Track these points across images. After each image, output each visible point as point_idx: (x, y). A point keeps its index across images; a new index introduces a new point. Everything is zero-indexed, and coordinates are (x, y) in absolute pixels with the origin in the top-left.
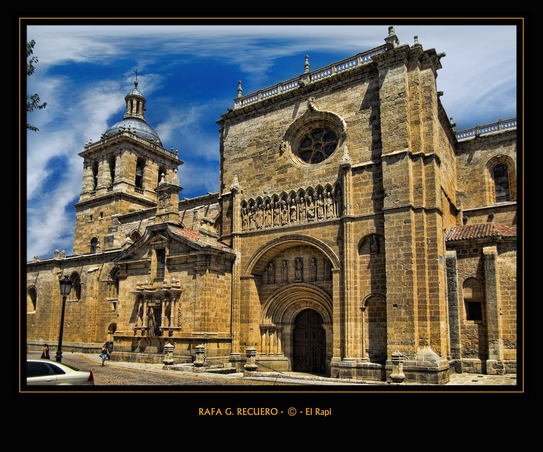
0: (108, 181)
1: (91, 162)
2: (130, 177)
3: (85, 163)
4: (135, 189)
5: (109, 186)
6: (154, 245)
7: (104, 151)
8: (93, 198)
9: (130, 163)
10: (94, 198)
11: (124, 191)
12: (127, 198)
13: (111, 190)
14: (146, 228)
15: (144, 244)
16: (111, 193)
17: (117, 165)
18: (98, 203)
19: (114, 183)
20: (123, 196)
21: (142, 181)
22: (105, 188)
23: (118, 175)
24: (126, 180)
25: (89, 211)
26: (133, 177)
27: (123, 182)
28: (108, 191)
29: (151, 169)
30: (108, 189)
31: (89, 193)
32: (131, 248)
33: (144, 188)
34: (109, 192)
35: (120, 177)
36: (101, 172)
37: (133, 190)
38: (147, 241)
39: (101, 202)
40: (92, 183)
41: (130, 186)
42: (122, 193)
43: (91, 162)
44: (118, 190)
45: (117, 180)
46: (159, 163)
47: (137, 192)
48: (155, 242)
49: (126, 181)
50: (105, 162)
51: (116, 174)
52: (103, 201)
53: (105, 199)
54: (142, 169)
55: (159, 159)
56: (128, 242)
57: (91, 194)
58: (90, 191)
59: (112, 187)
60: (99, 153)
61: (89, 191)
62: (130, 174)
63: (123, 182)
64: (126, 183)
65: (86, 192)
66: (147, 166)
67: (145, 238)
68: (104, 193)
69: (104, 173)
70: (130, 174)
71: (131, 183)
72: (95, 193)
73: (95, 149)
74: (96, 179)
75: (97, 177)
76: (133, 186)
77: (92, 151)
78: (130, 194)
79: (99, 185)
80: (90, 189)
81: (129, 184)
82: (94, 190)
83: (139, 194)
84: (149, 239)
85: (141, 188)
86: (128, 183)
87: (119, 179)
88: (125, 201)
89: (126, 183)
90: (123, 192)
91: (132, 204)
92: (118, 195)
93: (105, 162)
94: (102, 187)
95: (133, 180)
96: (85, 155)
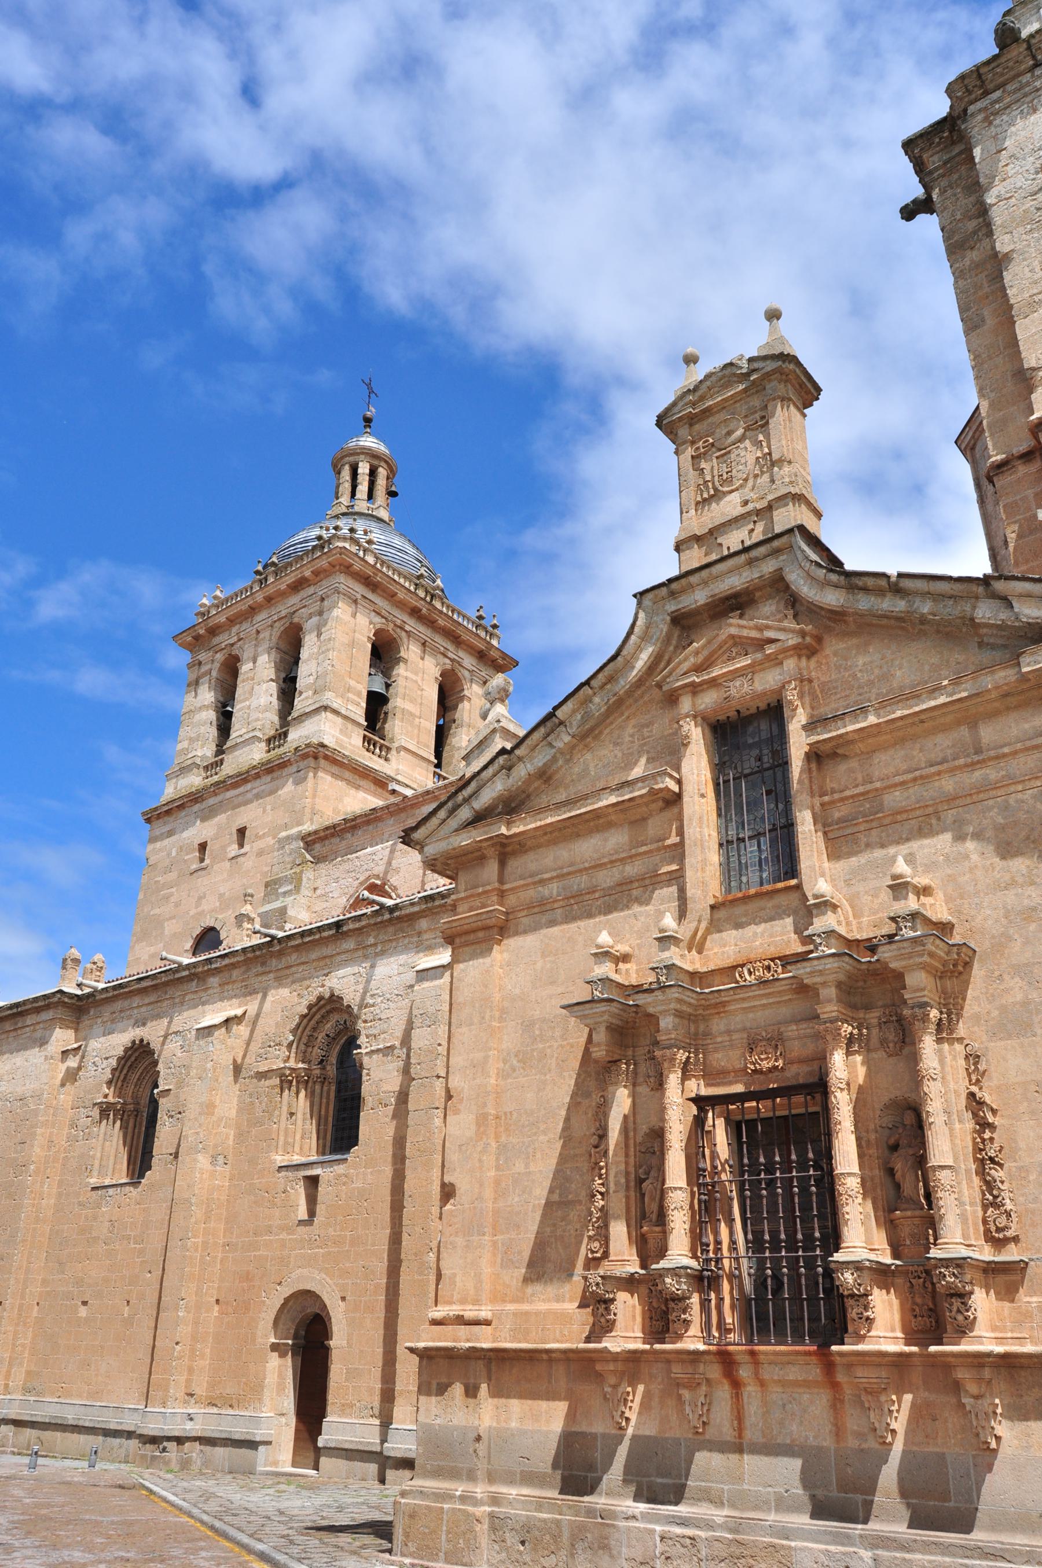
0: (268, 715)
2: (350, 695)
4: (365, 737)
5: (272, 733)
6: (695, 689)
9: (352, 644)
11: (328, 741)
12: (335, 769)
14: (639, 604)
17: (304, 654)
20: (326, 757)
22: (259, 740)
23: (308, 687)
25: (197, 831)
26: (359, 694)
27: (326, 708)
28: (269, 751)
29: (416, 674)
30: (269, 741)
31: (198, 766)
32: (537, 736)
33: (392, 740)
34: (272, 752)
35: (315, 692)
36: (247, 688)
38: (640, 682)
39: (241, 789)
40: (213, 732)
41: (350, 726)
42: (323, 745)
45: (302, 703)
46: (440, 656)
47: (368, 750)
48: (698, 669)
49: (335, 706)
52: (249, 786)
53: (257, 776)
54: (387, 673)
55: (441, 642)
57: (206, 768)
58: (203, 757)
59: (285, 734)
61: (198, 761)
62: (353, 683)
63: (326, 708)
64: (336, 712)
65: (189, 762)
66: (406, 661)
67: (629, 665)
68: (257, 754)
69: (256, 687)
70: (353, 683)
71: (352, 716)
76: (359, 724)
79: (238, 730)
80: (206, 751)
81: (346, 718)
83: (375, 758)
86: (343, 712)
87: (310, 701)
88: (329, 778)
89: (336, 712)
90: (326, 742)
94: (247, 737)
95: (358, 704)
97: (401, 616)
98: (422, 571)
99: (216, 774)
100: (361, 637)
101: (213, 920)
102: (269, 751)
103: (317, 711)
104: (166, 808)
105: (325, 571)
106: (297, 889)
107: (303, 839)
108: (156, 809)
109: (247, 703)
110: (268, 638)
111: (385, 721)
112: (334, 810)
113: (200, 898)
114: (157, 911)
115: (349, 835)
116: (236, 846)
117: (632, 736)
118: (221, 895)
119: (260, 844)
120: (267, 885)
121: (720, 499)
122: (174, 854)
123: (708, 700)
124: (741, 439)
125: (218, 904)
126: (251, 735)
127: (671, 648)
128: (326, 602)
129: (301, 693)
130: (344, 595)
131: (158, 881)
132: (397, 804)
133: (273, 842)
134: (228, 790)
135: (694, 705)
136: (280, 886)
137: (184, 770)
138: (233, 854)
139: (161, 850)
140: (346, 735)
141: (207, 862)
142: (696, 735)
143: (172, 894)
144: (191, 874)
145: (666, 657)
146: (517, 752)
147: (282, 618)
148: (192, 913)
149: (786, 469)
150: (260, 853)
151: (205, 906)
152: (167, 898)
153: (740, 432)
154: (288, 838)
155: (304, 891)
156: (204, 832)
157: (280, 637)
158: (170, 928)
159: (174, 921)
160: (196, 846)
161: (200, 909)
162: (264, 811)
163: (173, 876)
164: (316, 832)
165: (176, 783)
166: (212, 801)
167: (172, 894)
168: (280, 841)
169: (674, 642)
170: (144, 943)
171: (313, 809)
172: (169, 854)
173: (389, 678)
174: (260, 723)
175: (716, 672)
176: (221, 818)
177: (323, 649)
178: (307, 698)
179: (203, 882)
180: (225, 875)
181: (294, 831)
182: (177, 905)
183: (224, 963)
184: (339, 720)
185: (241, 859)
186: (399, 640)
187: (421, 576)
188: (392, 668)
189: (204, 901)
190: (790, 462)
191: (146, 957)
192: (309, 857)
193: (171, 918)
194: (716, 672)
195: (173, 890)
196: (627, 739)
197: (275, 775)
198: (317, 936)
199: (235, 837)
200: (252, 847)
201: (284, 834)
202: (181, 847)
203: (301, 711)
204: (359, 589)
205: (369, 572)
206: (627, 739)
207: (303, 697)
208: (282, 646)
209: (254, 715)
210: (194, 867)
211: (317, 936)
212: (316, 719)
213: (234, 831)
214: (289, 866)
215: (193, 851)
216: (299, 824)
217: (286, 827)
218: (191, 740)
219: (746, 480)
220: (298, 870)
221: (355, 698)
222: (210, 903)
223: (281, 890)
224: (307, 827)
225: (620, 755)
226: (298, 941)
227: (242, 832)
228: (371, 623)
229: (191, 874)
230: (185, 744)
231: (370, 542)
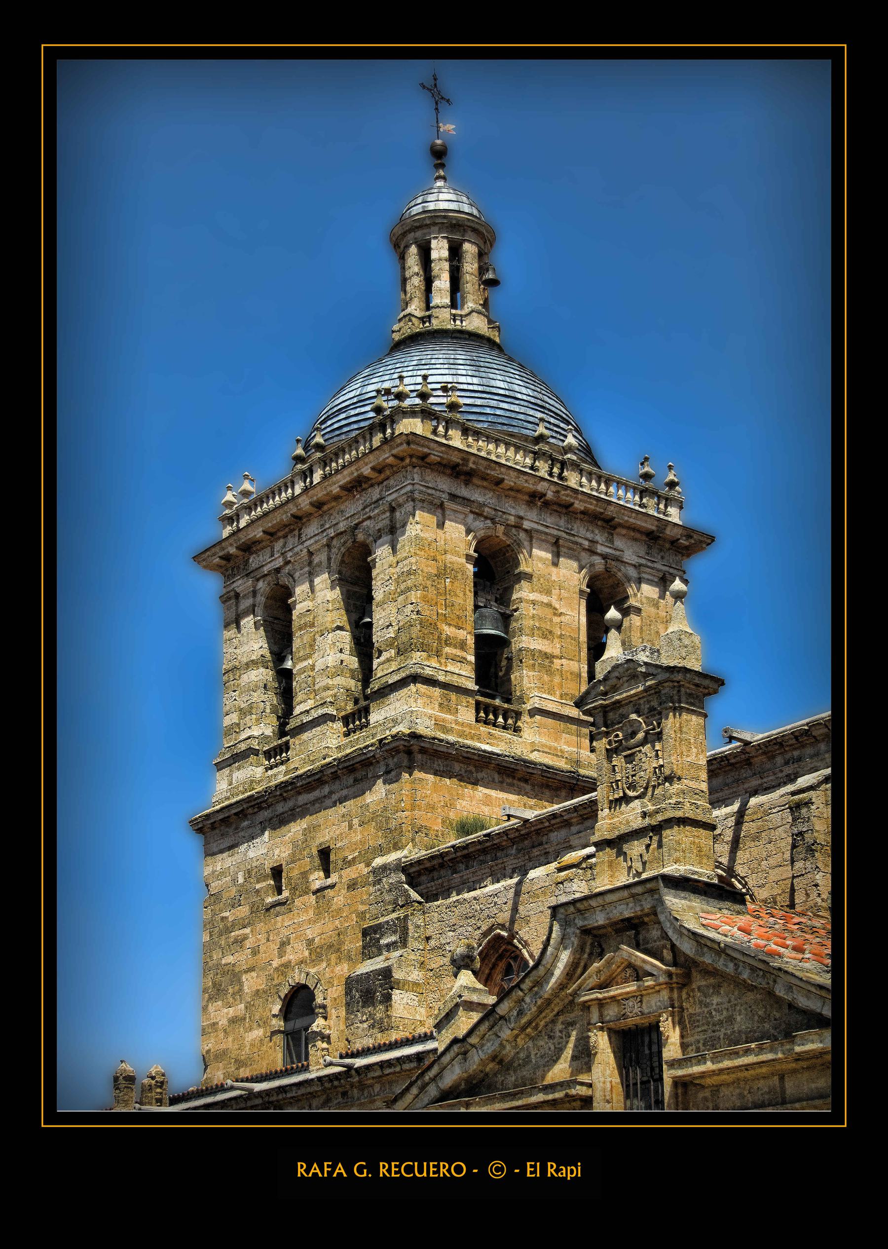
0: (339, 680)
1: (254, 593)
2: (447, 650)
3: (230, 598)
5: (350, 707)
7: (312, 529)
8: (280, 775)
10: (281, 778)
11: (425, 728)
12: (439, 764)
13: (361, 727)
15: (548, 1002)
16: (364, 740)
17: (378, 595)
18: (303, 798)
19: (375, 686)
20: (423, 751)
21: (509, 659)
22: (332, 718)
23: (390, 644)
24: (430, 667)
27: (415, 678)
28: (347, 734)
30: (346, 720)
31: (256, 753)
34: (354, 737)
35: (399, 653)
36: (306, 639)
37: (467, 714)
38: (561, 987)
39: (317, 794)
40: (272, 699)
41: (453, 696)
42: (414, 736)
43: (254, 593)
44: (395, 722)
48: (603, 986)
49: (428, 672)
50: (322, 580)
51: (378, 637)
52: (326, 790)
53: (335, 777)
56: (467, 996)
57: (268, 755)
58: (264, 738)
59: (366, 711)
60: (291, 541)
61: (255, 745)
62: (448, 630)
63: (415, 678)
64: (430, 682)
65: (243, 747)
67: (549, 973)
70: (448, 630)
72: (286, 747)
73: (268, 524)
74: (285, 677)
75: (288, 664)
76: (466, 692)
77: (258, 533)
78: (451, 738)
81: (445, 686)
82: (282, 732)
84: (571, 973)
85: (508, 701)
86: (441, 678)
87: (394, 666)
89: (430, 682)
90: (421, 730)
91: (468, 790)
92: (396, 750)
93: (322, 580)
94: (314, 714)
96: (227, 558)
97: (514, 510)
98: (541, 430)
99: (282, 763)
100: (455, 559)
101: (303, 975)
102: (347, 734)
103: (403, 683)
104: (221, 816)
105: (392, 466)
106: (403, 942)
107: (404, 870)
108: (208, 816)
109: (310, 661)
110: (325, 563)
111: (509, 669)
112: (443, 822)
113: (283, 944)
114: (230, 959)
115: (462, 866)
116: (322, 874)
117: (561, 1032)
118: (310, 942)
119: (350, 873)
120: (365, 933)
121: (627, 803)
122: (241, 880)
123: (612, 1012)
124: (643, 743)
125: (307, 953)
126: (320, 712)
127: (586, 956)
128: (398, 514)
129: (380, 653)
130: (423, 501)
131: (226, 918)
132: (517, 830)
133: (366, 871)
134: (299, 793)
135: (601, 1015)
136: (382, 935)
137: (238, 758)
138: (317, 885)
139: (223, 873)
140: (449, 711)
141: (286, 894)
142: (601, 1041)
143: (245, 938)
144: (268, 910)
145: (582, 964)
146: (473, 1040)
147: (341, 533)
148: (275, 963)
149: (677, 786)
150: (352, 886)
151: (291, 956)
152: (240, 942)
153: (641, 735)
154: (384, 868)
155: (412, 944)
156: (277, 852)
157: (342, 562)
158: (251, 983)
159: (254, 974)
160: (268, 871)
161: (285, 959)
162: (350, 827)
163: (243, 911)
164: (419, 862)
165: (230, 775)
166: (280, 808)
167: (245, 938)
168: (374, 871)
169: (588, 950)
170: (220, 1003)
171: (413, 825)
172: (235, 880)
173: (508, 606)
174: (330, 692)
175: (614, 991)
176: (296, 828)
177: (403, 587)
178: (388, 660)
179: (283, 922)
180: (311, 913)
181: (392, 857)
182: (255, 952)
183: (300, 1092)
184: (437, 692)
185: (329, 893)
186: (515, 547)
187: (541, 438)
188: (509, 590)
189: (289, 949)
190: (679, 779)
191: (223, 1022)
192: (414, 895)
193: (251, 969)
194: (614, 991)
195: (247, 931)
196: (558, 1034)
197: (359, 775)
198: (398, 1069)
199: (317, 862)
200: (341, 877)
201: (378, 861)
202: (249, 872)
203: (384, 680)
204: (445, 484)
205: (455, 458)
206: (558, 1034)
207: (382, 658)
208: (347, 572)
209: (322, 682)
210: (269, 900)
211: (398, 1069)
212: (404, 691)
213: (315, 852)
214: (390, 907)
215: (265, 878)
216: (397, 847)
217: (381, 851)
218: (243, 713)
219: (646, 788)
220: (400, 913)
221: (458, 652)
222: (296, 952)
223: (383, 942)
224: (410, 853)
225: (552, 1048)
226: (378, 1073)
227: (325, 854)
228: (468, 531)
229: (268, 910)
230: (234, 718)
231: (453, 407)
